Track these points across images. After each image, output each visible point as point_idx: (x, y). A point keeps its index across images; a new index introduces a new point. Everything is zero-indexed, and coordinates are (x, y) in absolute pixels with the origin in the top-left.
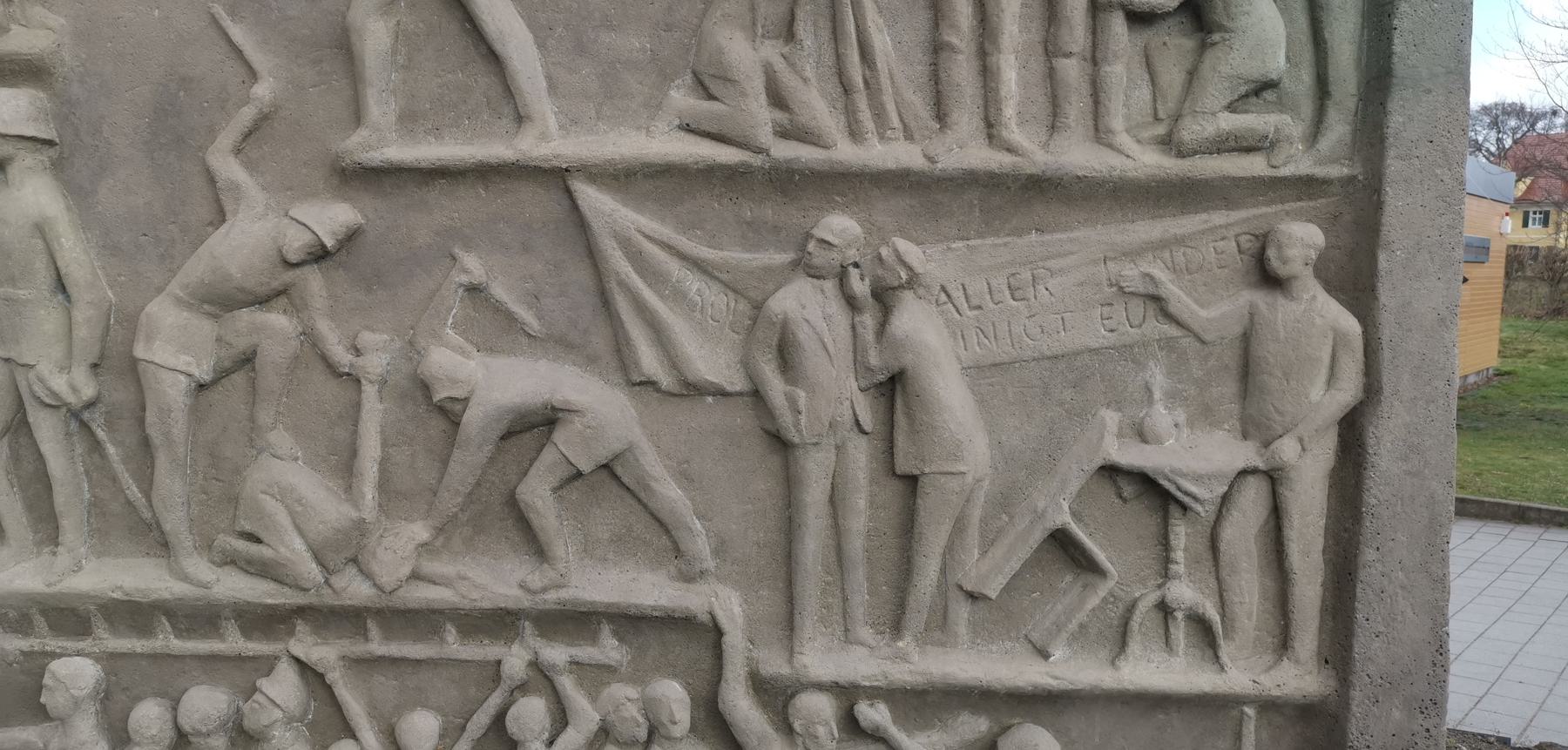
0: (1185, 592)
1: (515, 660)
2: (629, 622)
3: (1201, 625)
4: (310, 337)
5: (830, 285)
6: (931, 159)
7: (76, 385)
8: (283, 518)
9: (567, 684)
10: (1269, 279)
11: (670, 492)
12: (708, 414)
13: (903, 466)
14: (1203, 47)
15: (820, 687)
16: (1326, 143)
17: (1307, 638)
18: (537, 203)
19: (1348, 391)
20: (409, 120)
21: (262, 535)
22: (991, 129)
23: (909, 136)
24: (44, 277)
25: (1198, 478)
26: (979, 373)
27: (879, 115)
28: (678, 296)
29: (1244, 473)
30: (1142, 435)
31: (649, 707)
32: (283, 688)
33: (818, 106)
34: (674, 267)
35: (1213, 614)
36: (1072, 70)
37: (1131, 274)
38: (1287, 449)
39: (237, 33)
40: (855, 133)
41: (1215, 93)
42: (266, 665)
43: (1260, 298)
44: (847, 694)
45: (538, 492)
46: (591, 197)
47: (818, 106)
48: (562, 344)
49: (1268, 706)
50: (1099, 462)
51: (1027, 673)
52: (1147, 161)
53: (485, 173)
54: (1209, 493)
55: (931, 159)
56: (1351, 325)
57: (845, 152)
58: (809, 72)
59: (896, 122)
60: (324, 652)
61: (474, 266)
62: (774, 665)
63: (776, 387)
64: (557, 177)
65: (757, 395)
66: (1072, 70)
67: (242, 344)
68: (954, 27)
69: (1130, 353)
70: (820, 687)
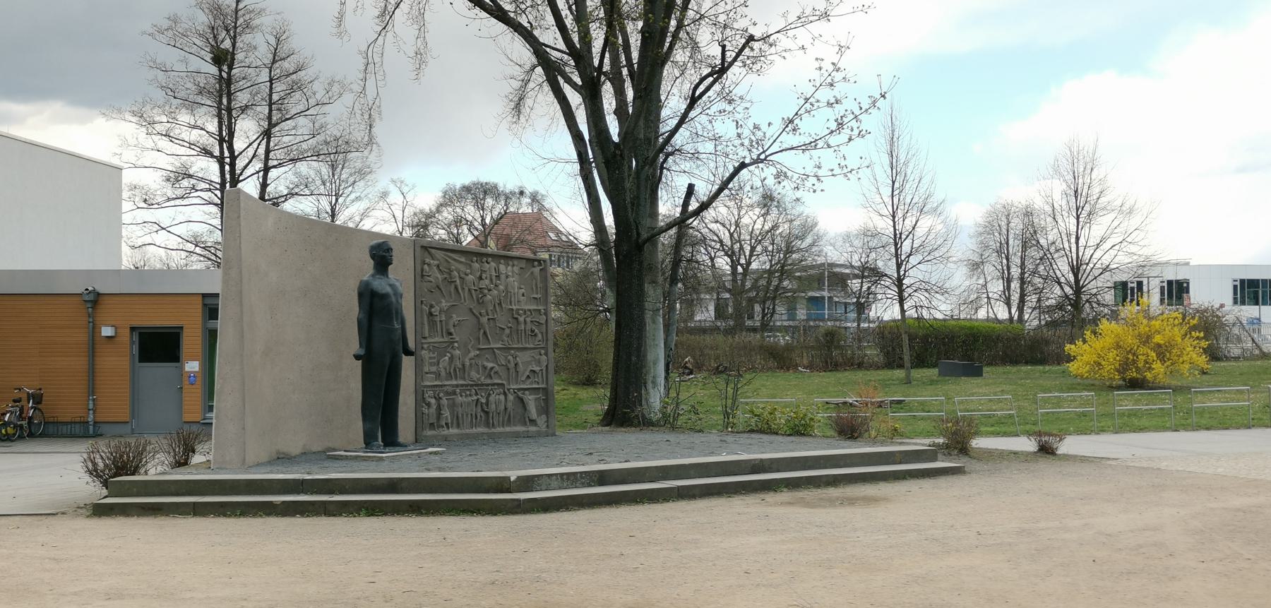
2: (498, 384)
7: (460, 366)
10: (541, 355)
18: (491, 351)
26: (522, 363)
33: (511, 343)
43: (539, 356)
44: (514, 389)
45: (492, 373)
46: (495, 350)
47: (511, 343)
48: (493, 362)
49: (543, 388)
51: (526, 387)
52: (532, 346)
53: (488, 348)
60: (476, 388)
61: (487, 356)
62: (509, 387)
63: (508, 365)
64: (492, 349)
69: (532, 361)
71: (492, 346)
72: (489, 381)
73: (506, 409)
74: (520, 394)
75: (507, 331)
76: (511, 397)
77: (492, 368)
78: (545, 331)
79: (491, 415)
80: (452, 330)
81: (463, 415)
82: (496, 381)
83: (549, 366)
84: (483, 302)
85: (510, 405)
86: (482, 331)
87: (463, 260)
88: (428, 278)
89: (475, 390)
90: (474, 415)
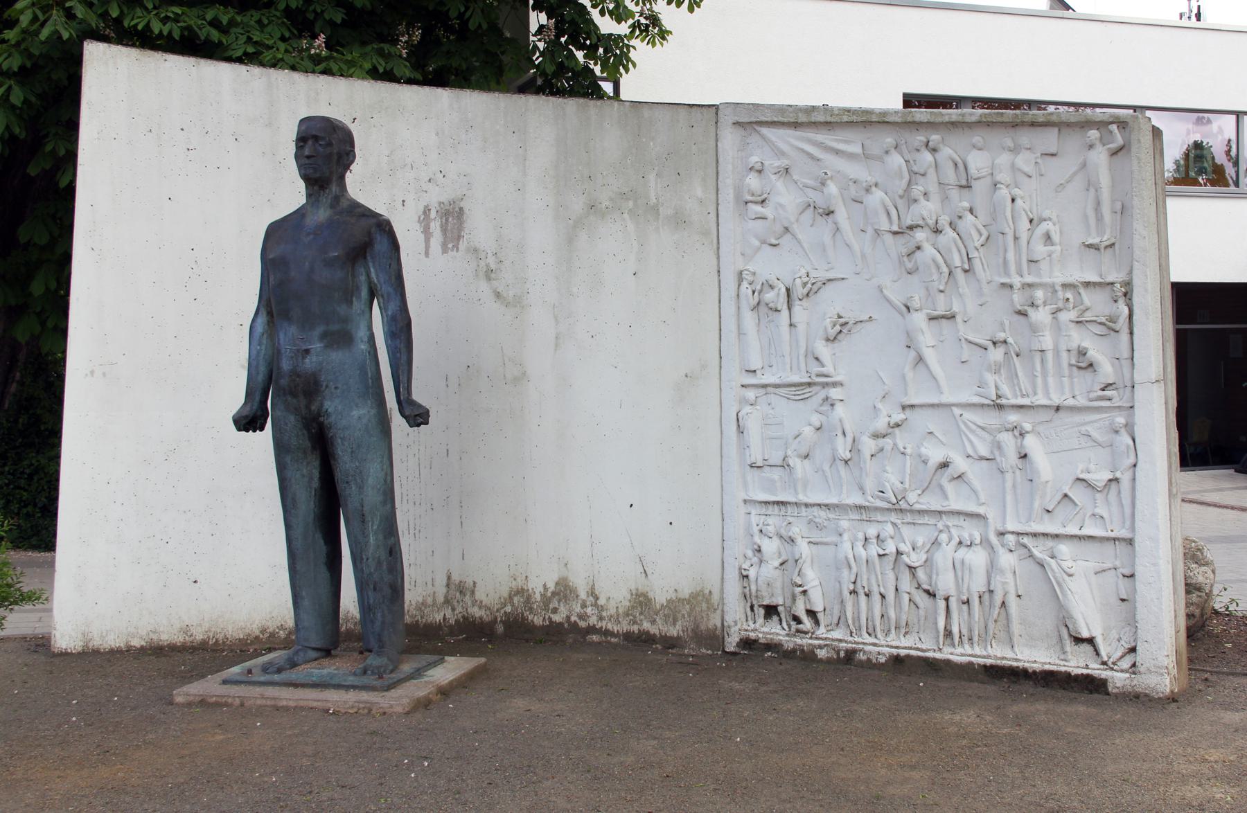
1: (940, 525)
4: (895, 444)
8: (889, 488)
9: (953, 531)
11: (977, 484)
21: (884, 491)
22: (1047, 393)
25: (1097, 481)
29: (1110, 480)
31: (971, 535)
32: (889, 529)
34: (974, 427)
35: (1105, 515)
37: (1083, 429)
39: (882, 374)
43: (1114, 436)
45: (944, 482)
57: (1013, 401)
67: (881, 446)
68: (1036, 371)
70: (1013, 533)
71: (946, 399)
78: (1126, 353)
82: (955, 506)
89: (894, 524)
90: (891, 596)
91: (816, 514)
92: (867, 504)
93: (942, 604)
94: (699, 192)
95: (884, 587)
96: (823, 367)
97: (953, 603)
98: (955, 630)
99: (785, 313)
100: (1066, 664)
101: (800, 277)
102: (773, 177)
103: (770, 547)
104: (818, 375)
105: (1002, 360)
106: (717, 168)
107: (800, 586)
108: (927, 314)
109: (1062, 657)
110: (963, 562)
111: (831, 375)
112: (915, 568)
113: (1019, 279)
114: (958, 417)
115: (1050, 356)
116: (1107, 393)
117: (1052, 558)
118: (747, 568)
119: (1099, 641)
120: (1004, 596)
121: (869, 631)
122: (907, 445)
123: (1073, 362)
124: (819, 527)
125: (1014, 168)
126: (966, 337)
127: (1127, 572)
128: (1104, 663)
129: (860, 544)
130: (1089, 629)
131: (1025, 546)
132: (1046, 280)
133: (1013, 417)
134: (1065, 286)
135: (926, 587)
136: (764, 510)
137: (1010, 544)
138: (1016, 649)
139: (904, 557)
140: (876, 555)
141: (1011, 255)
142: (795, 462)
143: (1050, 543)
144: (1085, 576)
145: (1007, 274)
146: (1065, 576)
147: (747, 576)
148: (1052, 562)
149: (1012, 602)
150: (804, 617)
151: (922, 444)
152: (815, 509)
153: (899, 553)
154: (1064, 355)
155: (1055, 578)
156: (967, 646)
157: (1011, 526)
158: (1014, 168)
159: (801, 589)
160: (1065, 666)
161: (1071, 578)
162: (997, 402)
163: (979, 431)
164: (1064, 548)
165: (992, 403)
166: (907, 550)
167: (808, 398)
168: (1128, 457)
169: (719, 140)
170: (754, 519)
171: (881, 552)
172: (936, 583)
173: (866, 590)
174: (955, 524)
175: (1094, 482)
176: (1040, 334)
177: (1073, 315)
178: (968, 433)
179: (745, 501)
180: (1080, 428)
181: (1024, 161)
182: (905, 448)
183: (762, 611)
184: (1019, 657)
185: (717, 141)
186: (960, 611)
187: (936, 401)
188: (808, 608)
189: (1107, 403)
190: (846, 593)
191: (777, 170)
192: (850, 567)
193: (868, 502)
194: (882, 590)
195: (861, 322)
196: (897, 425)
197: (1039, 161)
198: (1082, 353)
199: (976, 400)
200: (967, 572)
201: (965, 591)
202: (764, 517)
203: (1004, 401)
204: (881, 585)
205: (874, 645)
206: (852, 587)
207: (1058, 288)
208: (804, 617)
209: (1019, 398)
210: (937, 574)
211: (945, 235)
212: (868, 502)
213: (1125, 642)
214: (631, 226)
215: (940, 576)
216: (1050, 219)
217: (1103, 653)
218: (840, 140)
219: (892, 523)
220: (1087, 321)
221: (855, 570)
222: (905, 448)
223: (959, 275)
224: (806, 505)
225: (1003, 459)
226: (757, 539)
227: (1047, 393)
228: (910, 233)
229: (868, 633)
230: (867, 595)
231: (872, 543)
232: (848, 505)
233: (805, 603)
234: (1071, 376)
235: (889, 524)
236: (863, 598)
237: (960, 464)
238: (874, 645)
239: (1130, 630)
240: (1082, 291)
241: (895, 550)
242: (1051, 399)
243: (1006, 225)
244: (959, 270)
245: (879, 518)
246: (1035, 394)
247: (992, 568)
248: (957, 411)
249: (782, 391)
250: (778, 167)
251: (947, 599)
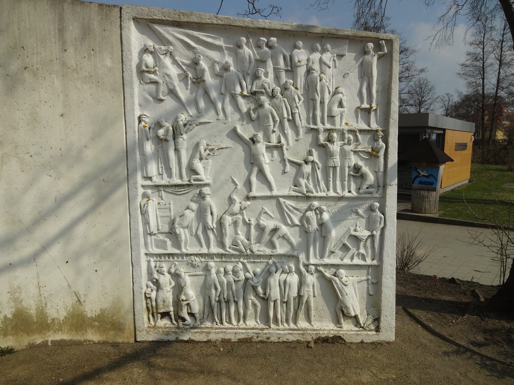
0: (362, 251)
1: (271, 262)
3: (363, 255)
5: (314, 211)
6: (327, 195)
9: (278, 265)
12: (297, 228)
13: (323, 235)
14: (362, 180)
15: (313, 265)
16: (379, 193)
17: (377, 257)
19: (382, 225)
20: (257, 190)
22: (335, 190)
23: (324, 192)
24: (210, 212)
25: (363, 236)
27: (320, 189)
28: (293, 212)
30: (355, 230)
32: (240, 265)
33: (311, 186)
36: (346, 183)
38: (375, 233)
39: (235, 180)
40: (317, 192)
41: (365, 187)
42: (237, 262)
44: (316, 265)
46: (282, 200)
50: (350, 234)
54: (365, 238)
55: (327, 195)
56: (382, 216)
57: (315, 194)
58: (311, 184)
59: (322, 190)
64: (276, 198)
65: (303, 225)
66: (346, 183)
67: (235, 220)
68: (330, 178)
70: (313, 265)
71: (275, 193)
72: (268, 251)
73: (300, 296)
74: (328, 274)
75: (307, 169)
76: (311, 279)
77: (275, 230)
79: (272, 304)
80: (199, 165)
81: (219, 302)
83: (387, 233)
84: (258, 118)
85: (308, 292)
86: (255, 170)
87: (220, 42)
88: (152, 76)
91: (193, 259)
92: (226, 253)
93: (272, 304)
94: (108, 63)
95: (237, 297)
96: (198, 175)
97: (279, 302)
98: (279, 316)
99: (172, 143)
100: (341, 329)
101: (182, 120)
102: (162, 57)
103: (166, 280)
104: (194, 180)
105: (310, 172)
106: (122, 47)
107: (186, 300)
108: (266, 145)
109: (339, 326)
110: (285, 282)
111: (203, 180)
112: (257, 287)
113: (323, 126)
114: (282, 203)
115: (338, 169)
116: (371, 190)
117: (335, 276)
118: (149, 293)
119: (359, 316)
120: (308, 297)
121: (227, 321)
122: (251, 219)
123: (352, 173)
124: (193, 266)
125: (321, 61)
126: (288, 158)
127: (374, 281)
128: (363, 328)
129: (222, 275)
130: (355, 312)
131: (320, 272)
132: (338, 127)
133: (316, 204)
134: (351, 131)
135: (262, 295)
136: (159, 258)
137: (313, 271)
138: (313, 323)
139: (250, 281)
140: (233, 281)
141: (318, 113)
142: (179, 230)
143: (333, 270)
144: (353, 285)
145: (315, 123)
146: (344, 286)
147: (150, 298)
148: (336, 279)
149: (312, 299)
150: (187, 317)
151: (260, 218)
152: (192, 257)
153: (247, 279)
154: (347, 169)
155: (338, 288)
156: (285, 324)
157: (312, 261)
158: (321, 61)
159: (186, 302)
160: (341, 331)
161: (346, 287)
162: (307, 195)
163: (295, 211)
164: (342, 272)
165: (304, 195)
166: (251, 277)
167: (186, 193)
168: (380, 223)
169: (123, 29)
170: (153, 264)
171: (236, 279)
172: (269, 294)
173: (226, 300)
174: (279, 261)
175: (361, 237)
176: (335, 157)
177: (352, 147)
178: (288, 211)
179: (146, 254)
180: (352, 208)
181: (327, 57)
182: (249, 221)
183: (159, 316)
184: (315, 327)
185: (121, 29)
186: (282, 307)
187: (268, 194)
188: (189, 311)
189: (370, 195)
190: (213, 302)
191: (165, 52)
192: (216, 289)
193: (227, 251)
194: (236, 299)
195: (221, 148)
196: (245, 208)
197: (335, 59)
198: (357, 169)
199: (294, 194)
200: (287, 287)
201: (286, 297)
202: (158, 262)
203: (311, 195)
204: (235, 297)
205: (231, 329)
206: (217, 299)
207: (346, 132)
208: (187, 317)
209: (319, 192)
210: (270, 290)
211: (277, 98)
212: (227, 251)
213: (372, 316)
214: (57, 83)
215: (272, 290)
216: (342, 93)
217: (361, 322)
218: (208, 36)
219: (241, 262)
220: (360, 151)
221: (219, 289)
222: (249, 221)
223: (287, 124)
224: (187, 255)
225: (310, 226)
226: (156, 276)
227: (335, 190)
228: (254, 96)
229: (226, 322)
230: (226, 302)
231: (229, 274)
232: (214, 254)
233: (187, 309)
234: (349, 181)
235: (240, 263)
236: (224, 305)
237: (284, 229)
238: (231, 329)
239: (374, 309)
240: (358, 134)
241: (244, 278)
242: (338, 193)
243: (316, 95)
244: (286, 120)
245: (233, 260)
246: (328, 190)
247: (301, 284)
248: (282, 200)
249: (170, 190)
250: (165, 50)
251: (275, 301)
